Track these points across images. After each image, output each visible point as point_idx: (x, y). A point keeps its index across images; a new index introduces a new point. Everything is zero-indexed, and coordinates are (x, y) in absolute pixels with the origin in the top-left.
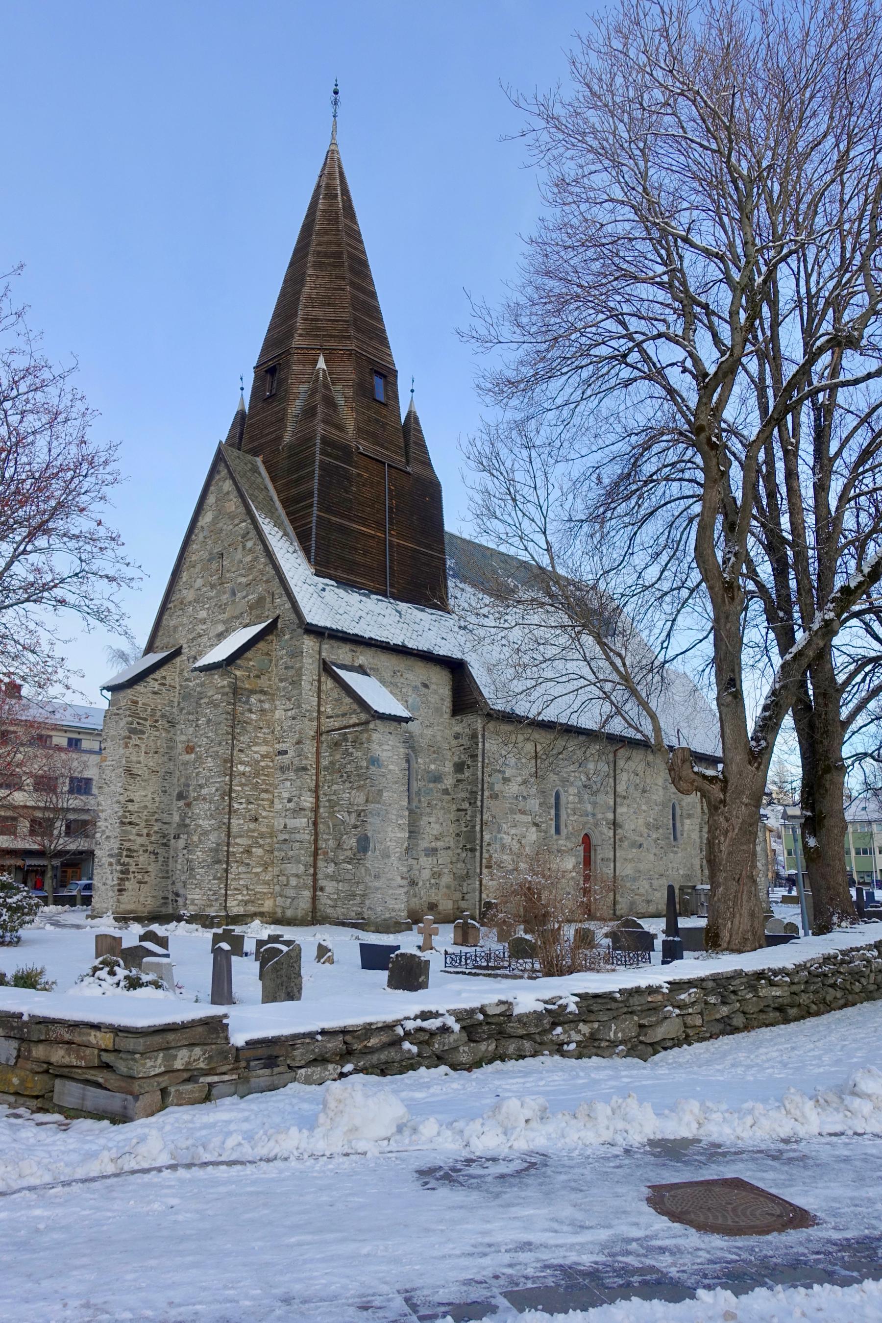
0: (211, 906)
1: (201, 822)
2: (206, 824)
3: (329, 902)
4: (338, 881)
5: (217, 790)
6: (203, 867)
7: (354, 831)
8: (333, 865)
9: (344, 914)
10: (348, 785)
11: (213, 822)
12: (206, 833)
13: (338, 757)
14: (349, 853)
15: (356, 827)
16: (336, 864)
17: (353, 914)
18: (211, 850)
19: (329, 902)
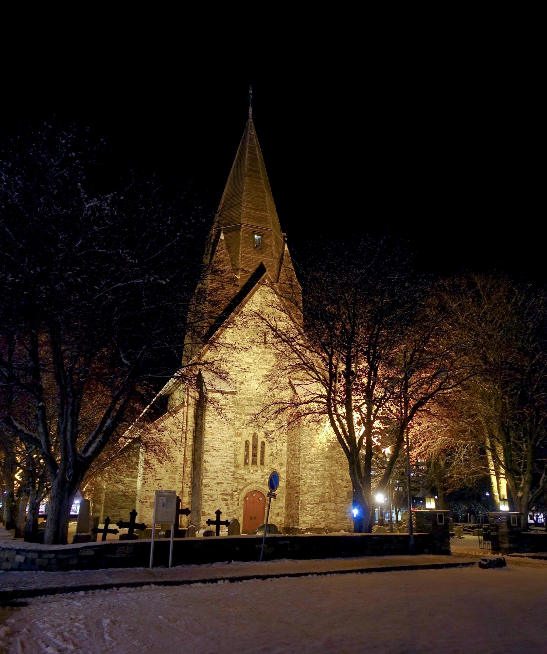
0: (320, 524)
1: (309, 481)
2: (313, 482)
3: (332, 521)
4: (336, 512)
5: (321, 466)
6: (313, 504)
7: (345, 489)
8: (334, 504)
9: (340, 527)
10: (340, 467)
11: (319, 481)
12: (313, 487)
13: (335, 454)
14: (343, 499)
15: (346, 487)
16: (336, 504)
17: (346, 527)
18: (318, 496)
19: (332, 521)
